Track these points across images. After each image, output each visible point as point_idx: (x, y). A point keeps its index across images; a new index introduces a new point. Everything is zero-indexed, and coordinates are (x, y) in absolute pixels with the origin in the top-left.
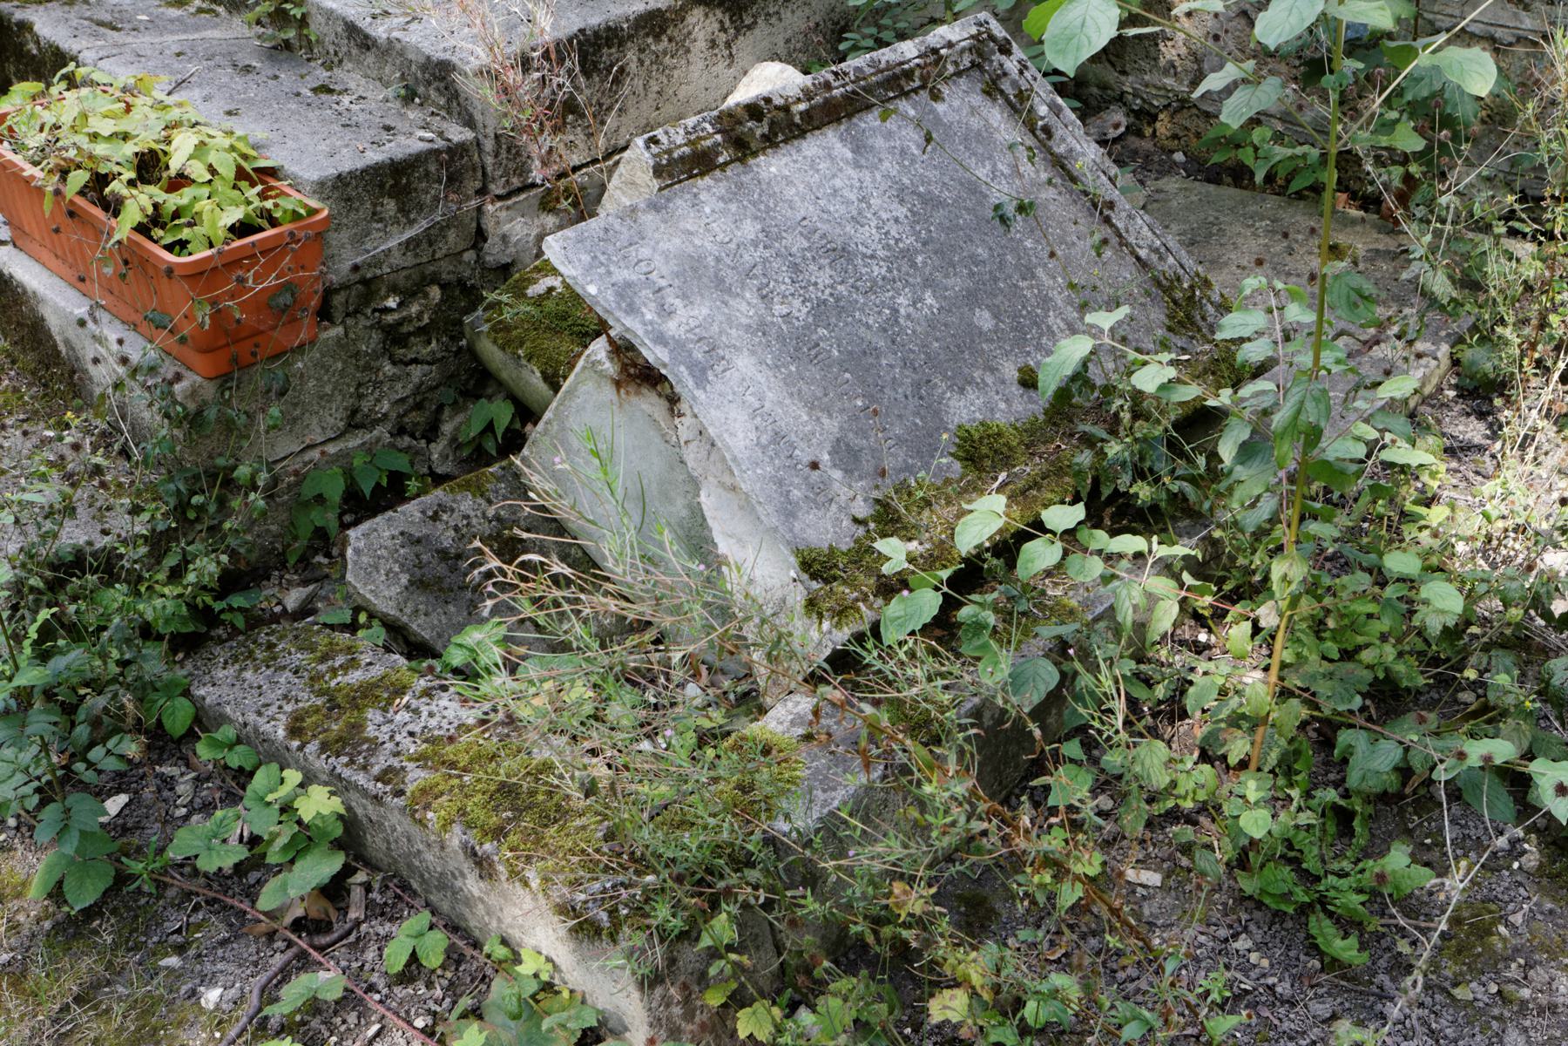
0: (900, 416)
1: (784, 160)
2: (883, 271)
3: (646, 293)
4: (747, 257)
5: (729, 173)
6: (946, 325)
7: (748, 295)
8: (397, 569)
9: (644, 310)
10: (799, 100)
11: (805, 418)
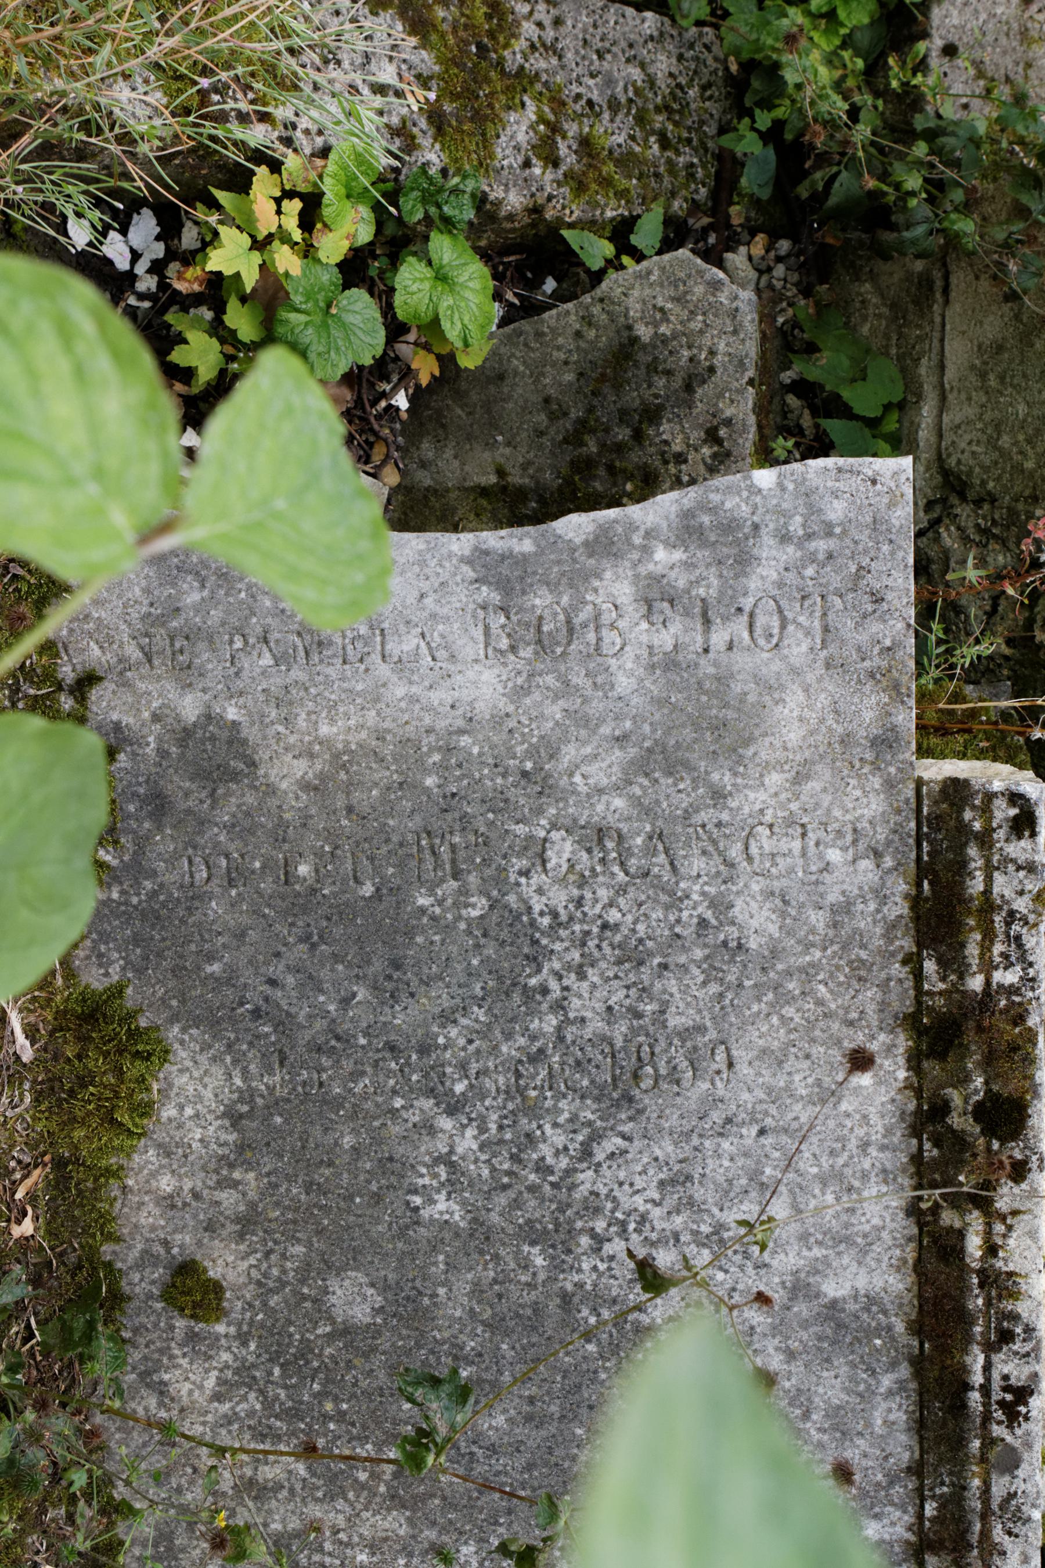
0: (241, 935)
1: (878, 1125)
2: (545, 1150)
3: (710, 588)
4: (698, 864)
5: (897, 970)
6: (377, 1198)
7: (619, 803)
8: (663, 329)
9: (678, 555)
10: (991, 1250)
11: (324, 730)
